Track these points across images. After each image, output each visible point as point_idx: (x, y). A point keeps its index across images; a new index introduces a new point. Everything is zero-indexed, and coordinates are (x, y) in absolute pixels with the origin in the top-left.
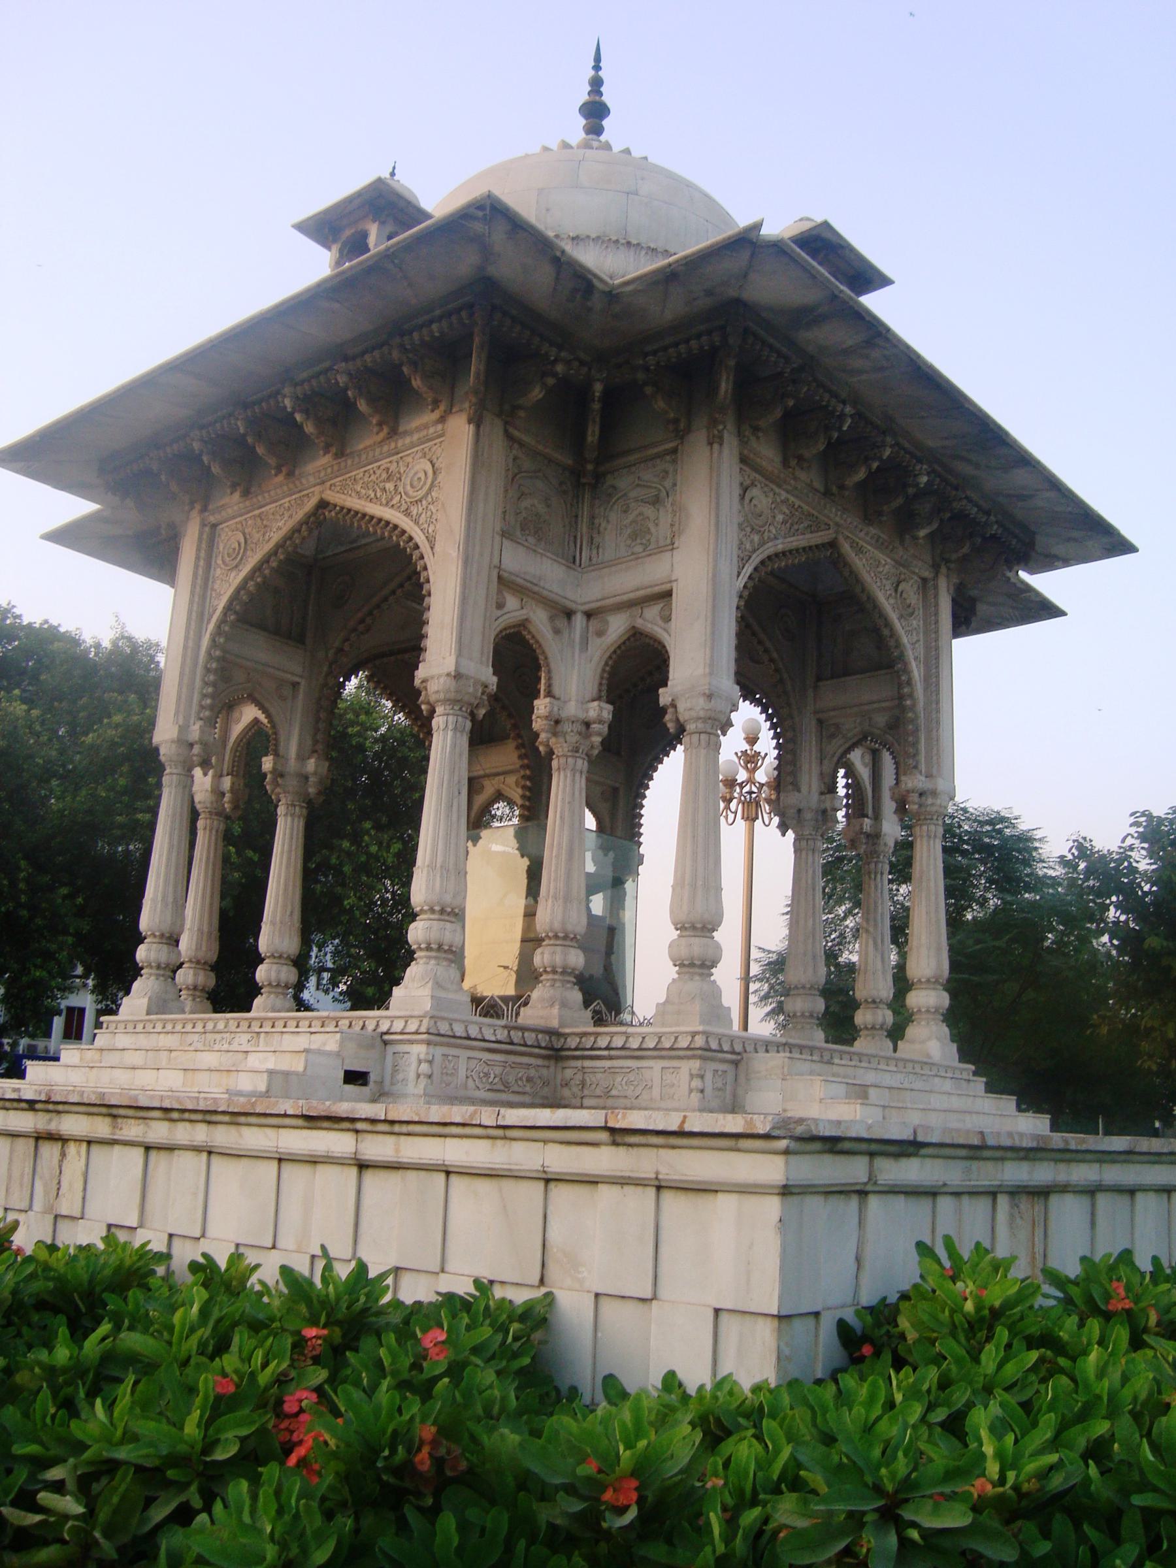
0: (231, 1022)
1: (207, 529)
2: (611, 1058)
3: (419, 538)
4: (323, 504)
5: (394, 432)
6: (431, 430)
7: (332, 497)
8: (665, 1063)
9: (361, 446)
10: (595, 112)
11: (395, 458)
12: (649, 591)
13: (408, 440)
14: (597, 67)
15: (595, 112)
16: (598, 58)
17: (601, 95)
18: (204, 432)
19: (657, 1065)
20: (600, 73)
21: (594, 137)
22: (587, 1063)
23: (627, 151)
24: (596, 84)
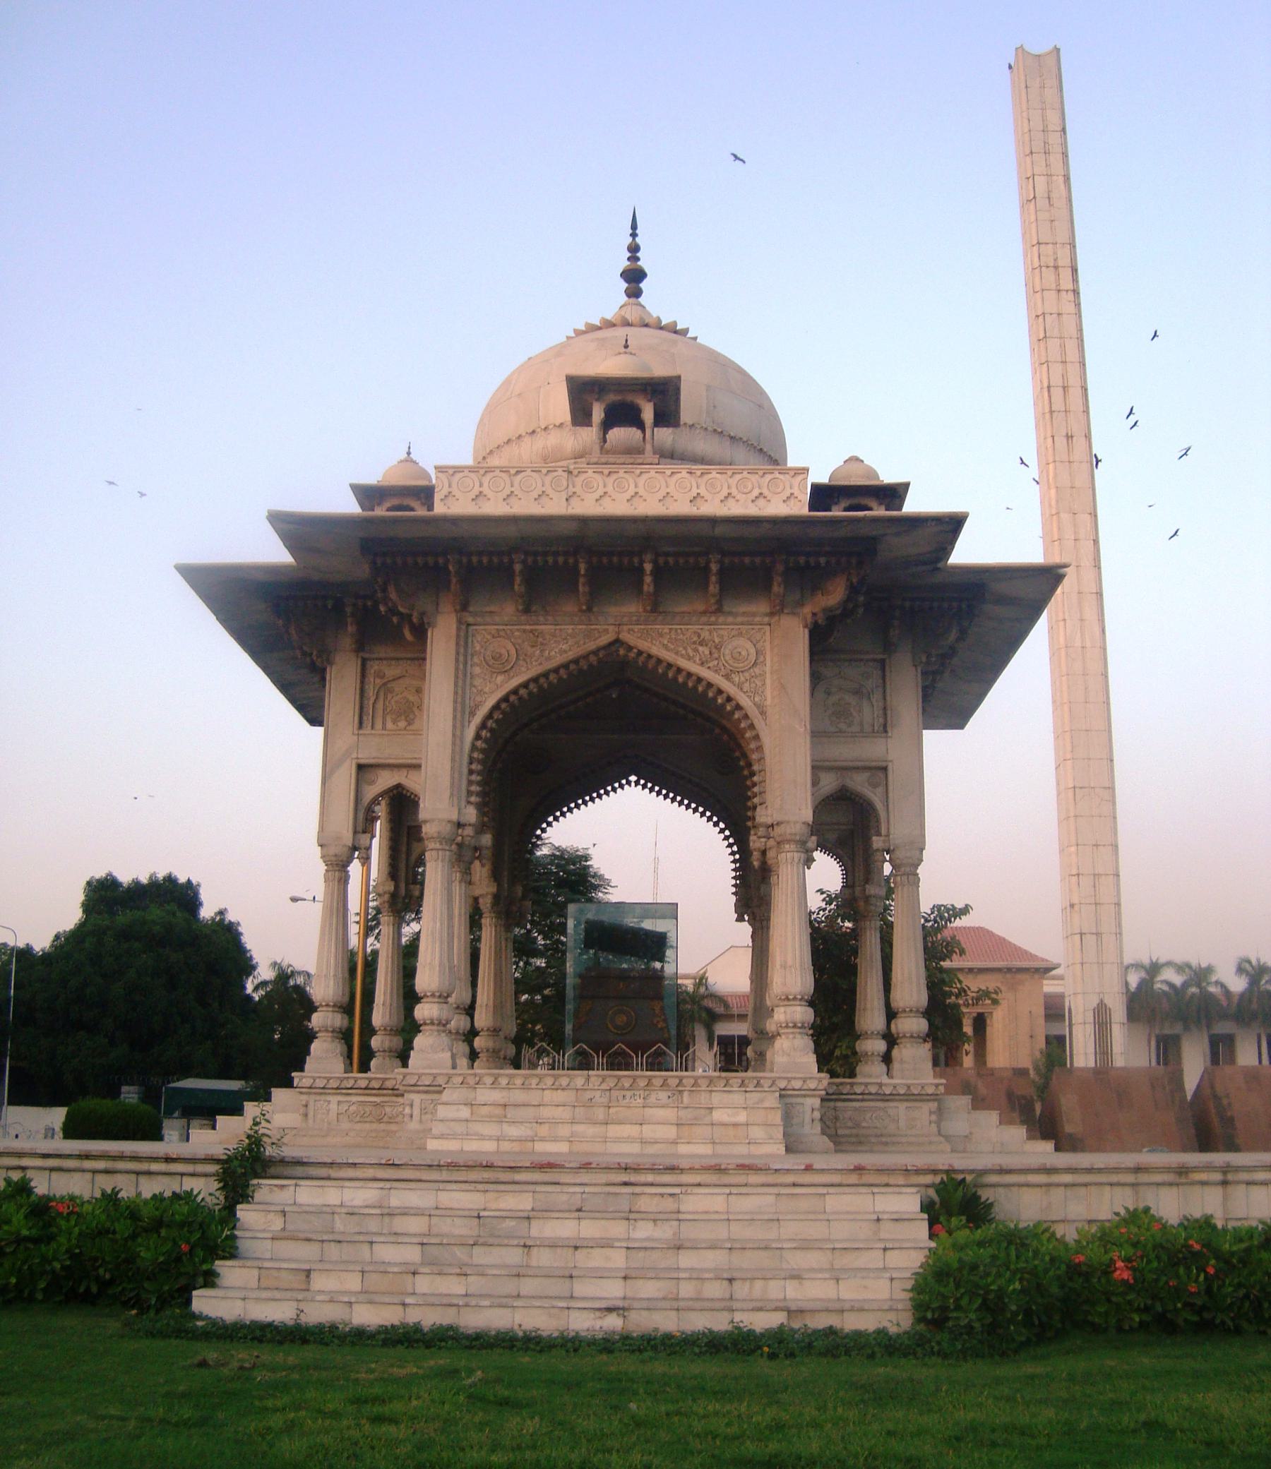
0: (592, 1079)
1: (464, 627)
2: (863, 1100)
3: (744, 701)
4: (617, 641)
5: (719, 610)
6: (757, 619)
7: (625, 636)
8: (909, 1104)
9: (678, 609)
10: (634, 277)
11: (707, 627)
12: (867, 764)
13: (730, 619)
14: (634, 235)
15: (634, 277)
16: (634, 226)
17: (638, 259)
18: (530, 560)
19: (902, 1106)
20: (637, 239)
21: (633, 300)
22: (839, 1104)
23: (695, 339)
24: (634, 249)
